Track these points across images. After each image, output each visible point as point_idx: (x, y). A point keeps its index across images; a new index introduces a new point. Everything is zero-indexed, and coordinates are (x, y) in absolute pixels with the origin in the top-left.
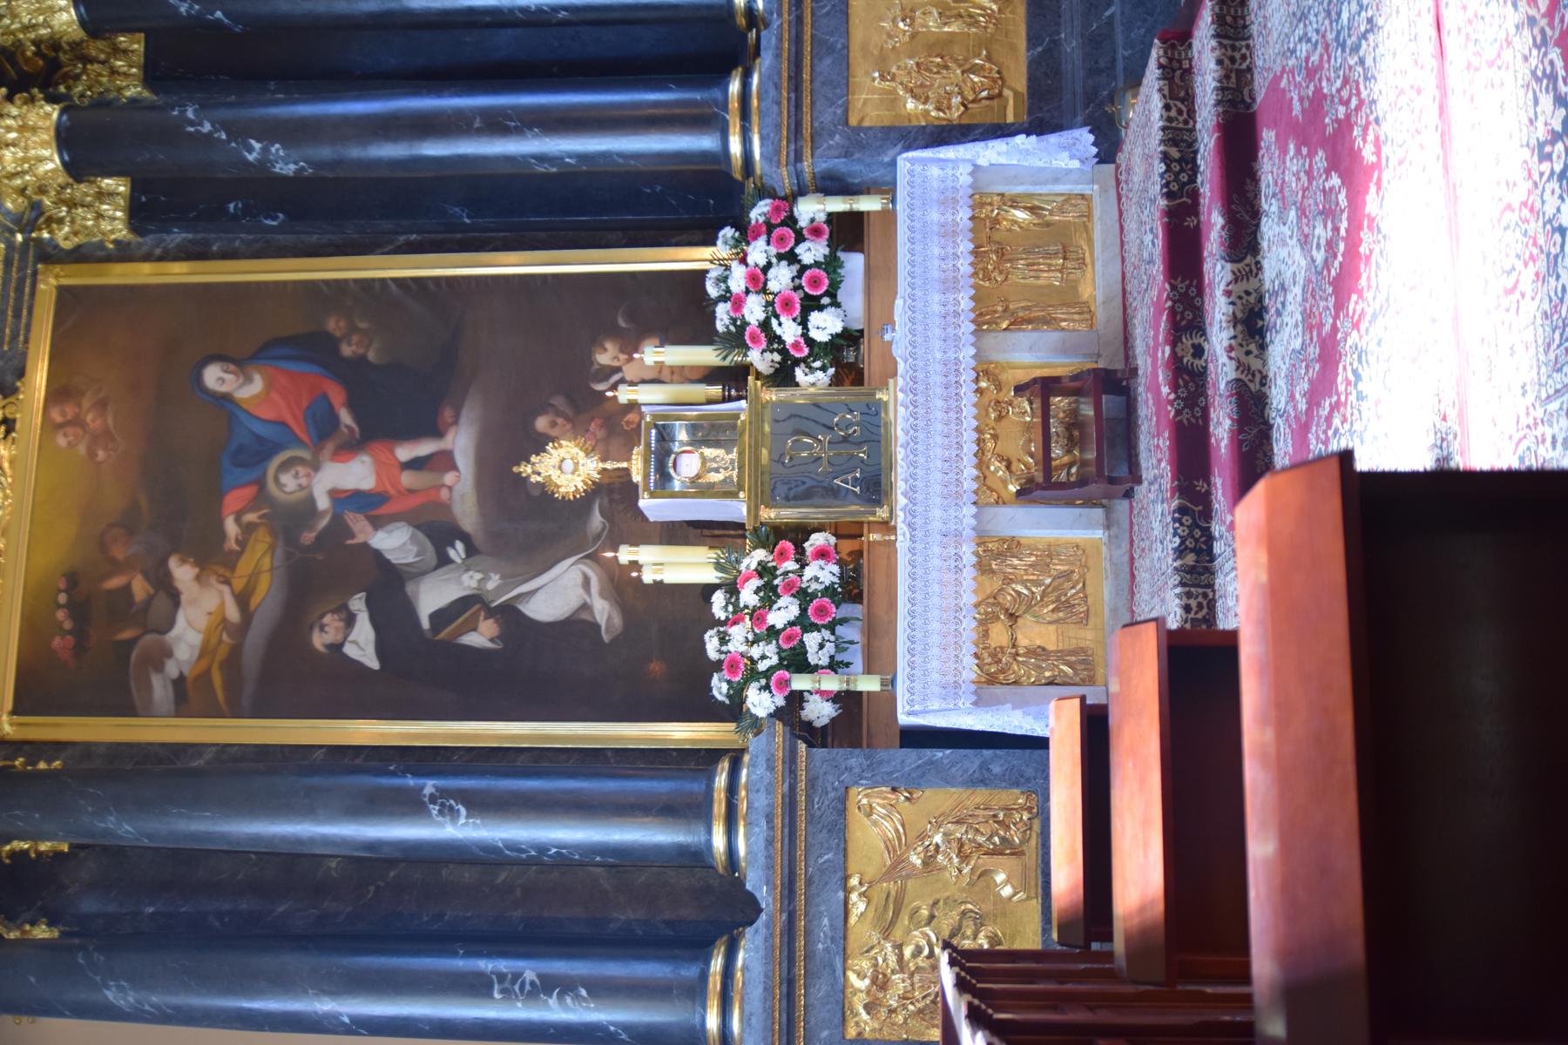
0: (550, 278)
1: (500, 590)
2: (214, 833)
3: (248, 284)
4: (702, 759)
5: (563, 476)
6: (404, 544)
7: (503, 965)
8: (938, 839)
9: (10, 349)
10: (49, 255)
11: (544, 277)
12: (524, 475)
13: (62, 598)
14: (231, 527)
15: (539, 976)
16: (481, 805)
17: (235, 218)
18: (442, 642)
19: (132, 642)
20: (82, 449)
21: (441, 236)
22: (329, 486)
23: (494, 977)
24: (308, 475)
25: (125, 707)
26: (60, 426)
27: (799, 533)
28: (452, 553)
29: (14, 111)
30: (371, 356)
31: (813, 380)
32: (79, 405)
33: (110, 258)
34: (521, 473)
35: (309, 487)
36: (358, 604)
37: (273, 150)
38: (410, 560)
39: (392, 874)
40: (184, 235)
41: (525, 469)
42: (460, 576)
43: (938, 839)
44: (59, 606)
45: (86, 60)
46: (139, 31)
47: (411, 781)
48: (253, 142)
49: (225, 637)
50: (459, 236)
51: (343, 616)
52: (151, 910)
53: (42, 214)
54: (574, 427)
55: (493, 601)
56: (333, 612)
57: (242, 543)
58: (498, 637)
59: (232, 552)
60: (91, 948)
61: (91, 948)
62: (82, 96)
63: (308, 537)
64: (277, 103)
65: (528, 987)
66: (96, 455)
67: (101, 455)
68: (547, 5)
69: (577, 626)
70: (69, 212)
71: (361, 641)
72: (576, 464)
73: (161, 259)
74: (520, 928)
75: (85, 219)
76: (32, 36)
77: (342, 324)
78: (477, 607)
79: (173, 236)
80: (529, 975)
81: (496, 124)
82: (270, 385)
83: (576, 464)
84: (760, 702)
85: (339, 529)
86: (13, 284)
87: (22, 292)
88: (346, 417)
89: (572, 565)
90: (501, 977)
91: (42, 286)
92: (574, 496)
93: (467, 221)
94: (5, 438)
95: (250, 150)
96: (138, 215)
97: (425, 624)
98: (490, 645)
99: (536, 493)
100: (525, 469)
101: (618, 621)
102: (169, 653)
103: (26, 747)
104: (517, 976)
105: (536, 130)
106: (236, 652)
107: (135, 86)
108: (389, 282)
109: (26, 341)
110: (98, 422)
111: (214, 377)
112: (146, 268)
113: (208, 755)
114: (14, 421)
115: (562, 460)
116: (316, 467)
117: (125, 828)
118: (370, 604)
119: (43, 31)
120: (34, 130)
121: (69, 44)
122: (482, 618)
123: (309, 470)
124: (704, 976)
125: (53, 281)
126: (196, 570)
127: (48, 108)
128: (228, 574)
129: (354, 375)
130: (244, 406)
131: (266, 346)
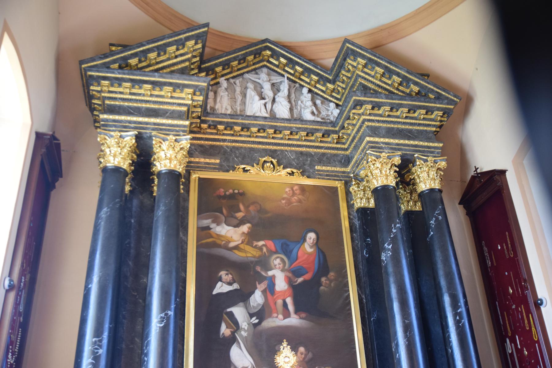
0: (354, 350)
1: (241, 336)
2: (157, 240)
3: (344, 246)
5: (283, 358)
6: (257, 302)
7: (105, 342)
9: (316, 174)
10: (347, 184)
11: (355, 348)
12: (283, 343)
13: (236, 191)
14: (261, 243)
15: (100, 355)
16: (164, 331)
17: (365, 241)
18: (222, 316)
19: (222, 213)
20: (285, 196)
21: (366, 310)
22: (276, 275)
23: (101, 338)
24: (280, 268)
25: (200, 211)
26: (292, 189)
28: (254, 318)
29: (392, 173)
30: (322, 288)
32: (299, 195)
33: (348, 202)
34: (284, 342)
35: (276, 268)
36: (236, 286)
37: (389, 252)
38: (251, 304)
39: (141, 301)
40: (358, 225)
41: (285, 344)
42: (246, 322)
44: (234, 190)
45: (411, 194)
46: (423, 209)
47: (173, 306)
48: (391, 245)
49: (224, 242)
50: (366, 316)
51: (231, 281)
52: (133, 221)
53: (360, 182)
54: (301, 361)
55: (237, 334)
56: (233, 278)
57: (256, 247)
58: (224, 336)
59: (253, 243)
60: (121, 203)
61: (121, 203)
62: (399, 193)
63: (258, 269)
64: (405, 252)
65: (96, 351)
66: (283, 200)
67: (284, 202)
68: (452, 345)
70: (362, 190)
71: (222, 288)
72: (288, 363)
73: (349, 218)
74: (118, 347)
75: (360, 194)
76: (416, 177)
77: (332, 277)
78: (235, 328)
79: (357, 221)
80: (100, 351)
81: (407, 328)
82: (310, 254)
83: (288, 363)
85: (262, 279)
86: (337, 174)
87: (335, 177)
88: (300, 280)
89: (251, 363)
90: (101, 341)
91: (337, 182)
92: (276, 362)
93: (372, 319)
94: (288, 173)
95: (389, 245)
96: (363, 211)
97: (229, 310)
98: (221, 333)
99: (277, 348)
100: (285, 344)
102: (218, 225)
103: (188, 182)
104: (101, 346)
105: (407, 343)
106: (219, 246)
107: (405, 208)
108: (348, 293)
109: (319, 178)
110: (294, 200)
111: (311, 236)
112: (346, 214)
113: (184, 238)
114: (293, 176)
115: (288, 357)
116: (282, 271)
117: (160, 212)
118: (236, 290)
119: (418, 180)
120: (387, 179)
121: (415, 188)
122: (231, 330)
123: (281, 268)
125: (339, 186)
126: (246, 232)
127: (394, 182)
128: (245, 243)
129: (315, 282)
130: (302, 246)
131: (323, 253)
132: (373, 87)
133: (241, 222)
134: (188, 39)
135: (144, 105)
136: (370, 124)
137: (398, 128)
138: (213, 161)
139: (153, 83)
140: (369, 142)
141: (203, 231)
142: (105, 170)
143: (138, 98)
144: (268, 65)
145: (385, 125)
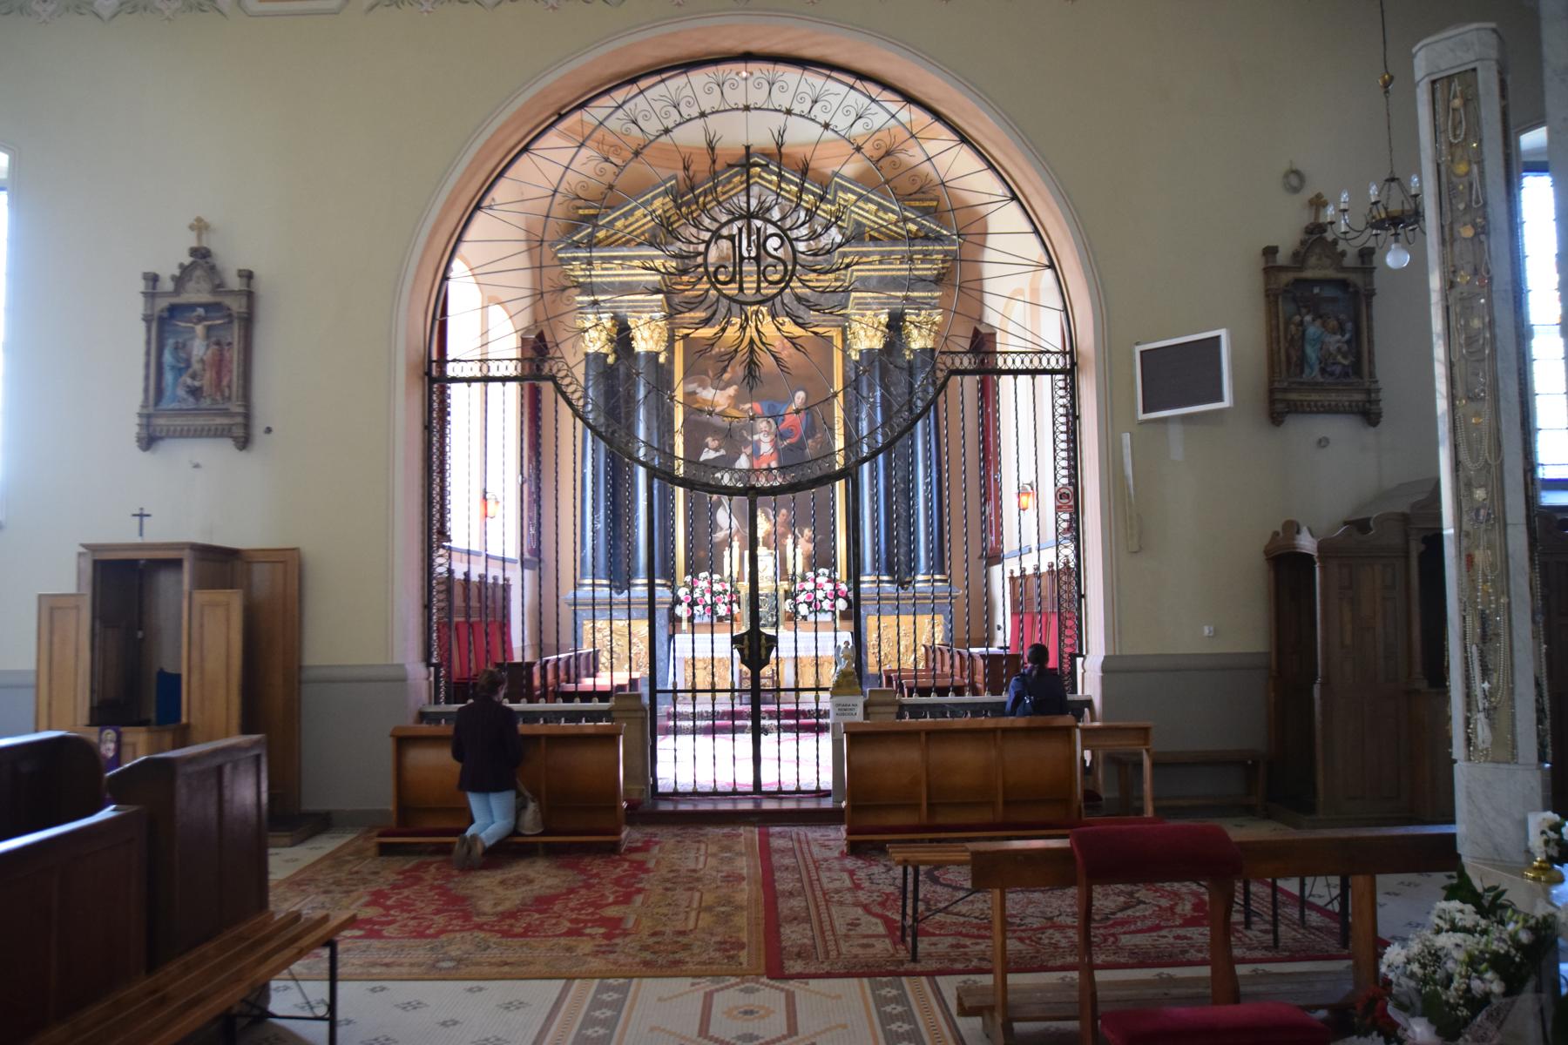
8: (641, 647)
13: (722, 350)
19: (708, 376)
31: (787, 606)
36: (722, 452)
43: (641, 647)
69: (714, 526)
85: (745, 442)
101: (717, 540)
118: (722, 456)
124: (600, 578)
125: (834, 334)
129: (800, 446)
132: (868, 223)
133: (728, 385)
134: (654, 198)
135: (617, 279)
136: (859, 273)
137: (892, 276)
139: (623, 258)
140: (855, 298)
141: (689, 395)
142: (587, 355)
143: (610, 272)
144: (760, 181)
145: (877, 273)
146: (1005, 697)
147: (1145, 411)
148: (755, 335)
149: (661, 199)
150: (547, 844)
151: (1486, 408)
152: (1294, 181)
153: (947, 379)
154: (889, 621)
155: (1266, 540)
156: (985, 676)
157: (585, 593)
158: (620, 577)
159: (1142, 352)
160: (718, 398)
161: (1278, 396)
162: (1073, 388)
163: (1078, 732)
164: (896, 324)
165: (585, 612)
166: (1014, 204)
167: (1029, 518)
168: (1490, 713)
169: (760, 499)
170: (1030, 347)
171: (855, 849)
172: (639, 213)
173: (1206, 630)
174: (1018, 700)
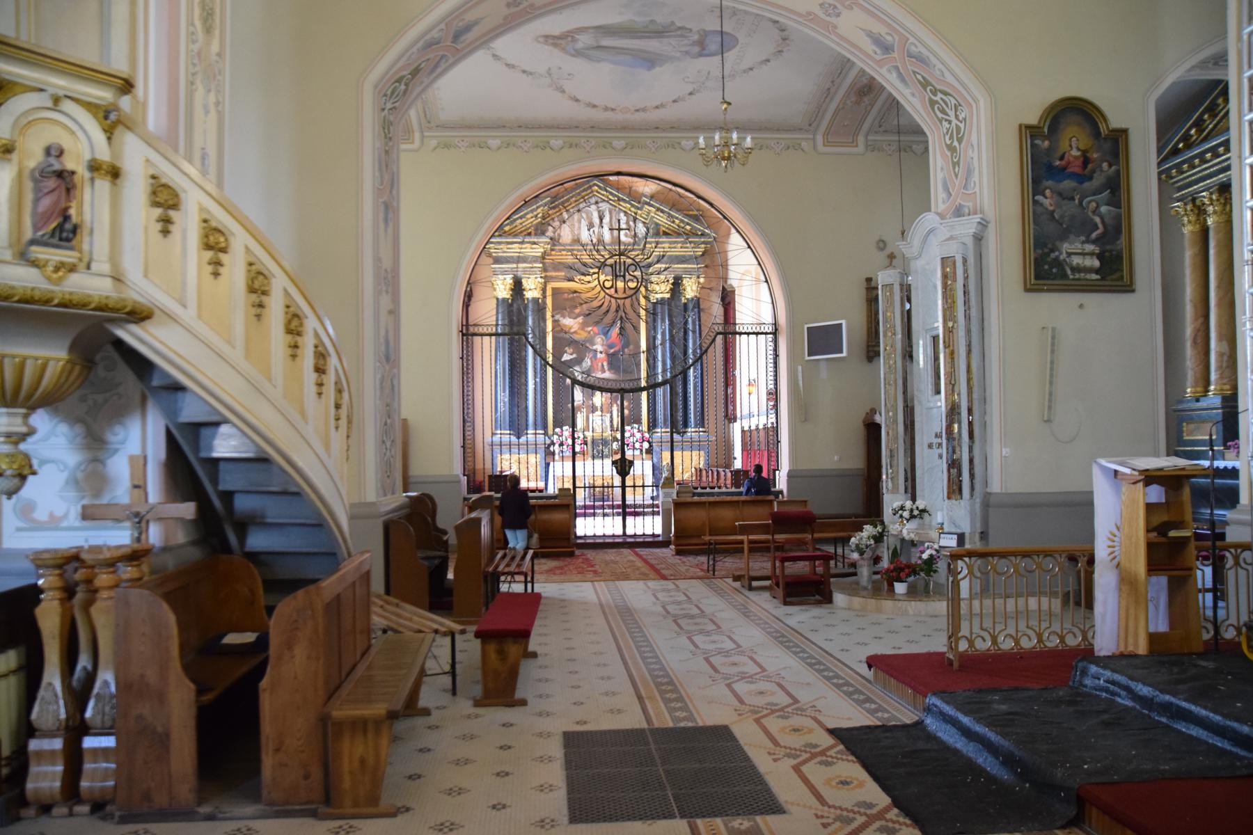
4: (545, 427)
14: (590, 329)
27: (586, 443)
36: (574, 356)
63: (588, 345)
84: (555, 438)
102: (564, 318)
134: (538, 208)
138: (560, 274)
141: (555, 322)
146: (741, 489)
147: (809, 355)
148: (624, 315)
149: (542, 208)
150: (542, 552)
151: (893, 388)
152: (881, 245)
153: (716, 337)
154: (687, 454)
155: (864, 416)
156: (732, 480)
157: (497, 439)
158: (517, 427)
159: (808, 328)
160: (571, 323)
161: (871, 349)
162: (776, 341)
163: (775, 503)
164: (677, 284)
165: (497, 449)
166: (749, 250)
167: (754, 397)
168: (892, 479)
169: (626, 395)
170: (755, 321)
171: (679, 553)
172: (529, 216)
173: (836, 458)
174: (748, 490)
